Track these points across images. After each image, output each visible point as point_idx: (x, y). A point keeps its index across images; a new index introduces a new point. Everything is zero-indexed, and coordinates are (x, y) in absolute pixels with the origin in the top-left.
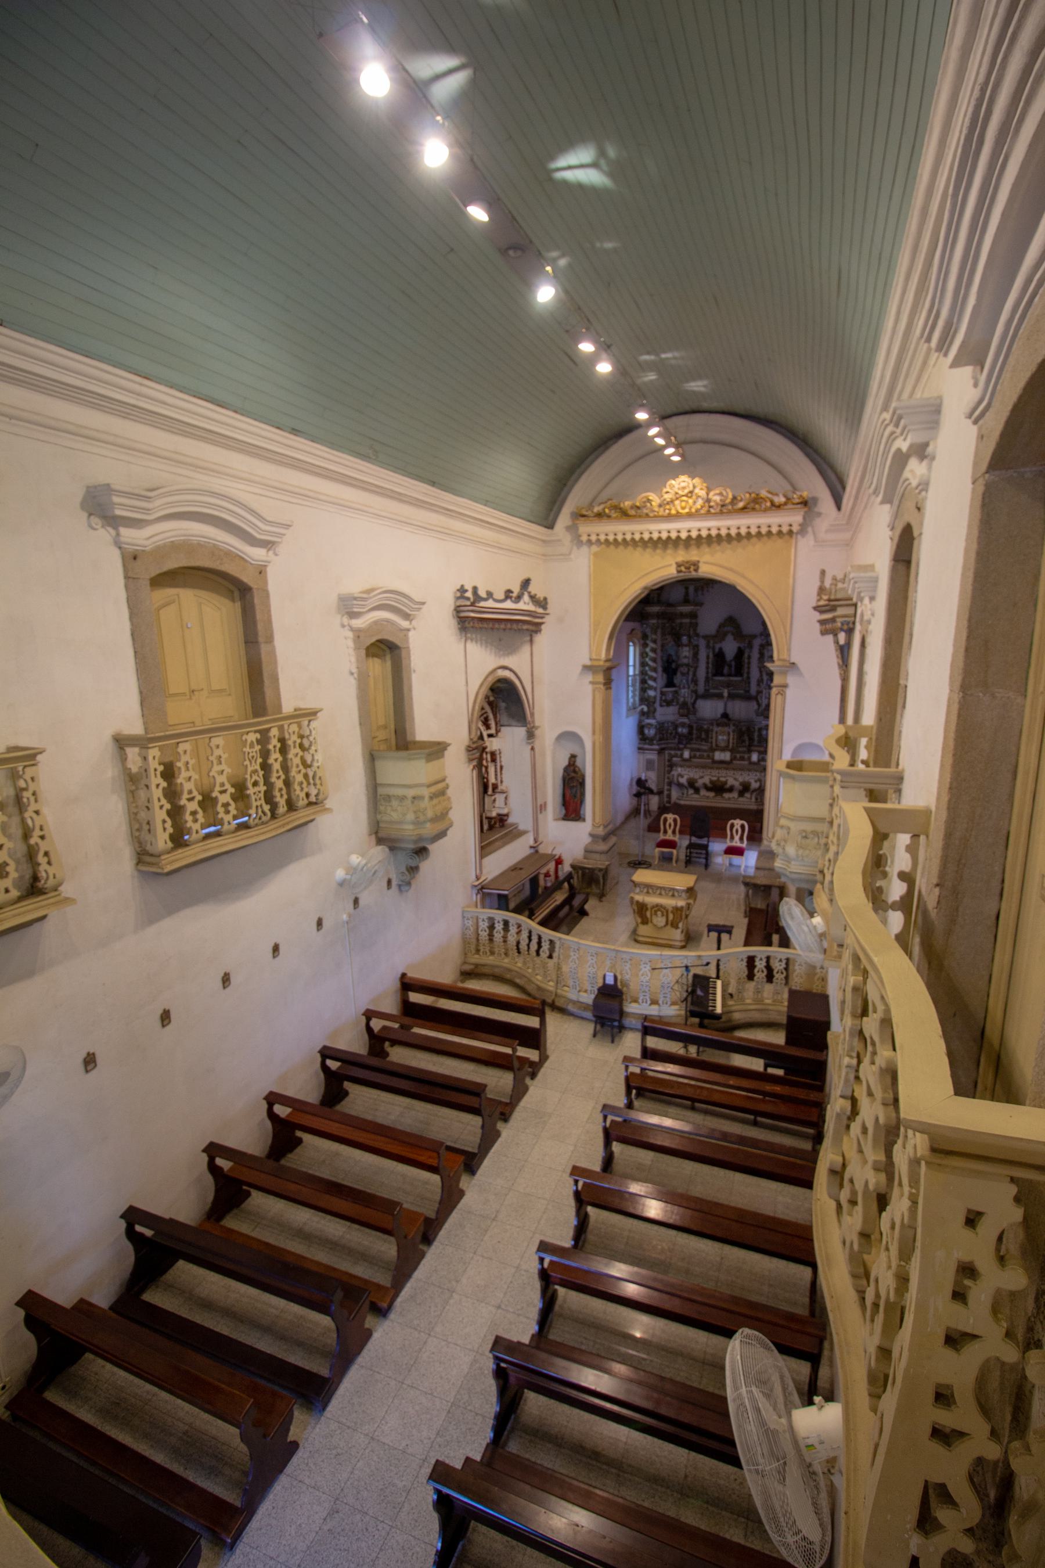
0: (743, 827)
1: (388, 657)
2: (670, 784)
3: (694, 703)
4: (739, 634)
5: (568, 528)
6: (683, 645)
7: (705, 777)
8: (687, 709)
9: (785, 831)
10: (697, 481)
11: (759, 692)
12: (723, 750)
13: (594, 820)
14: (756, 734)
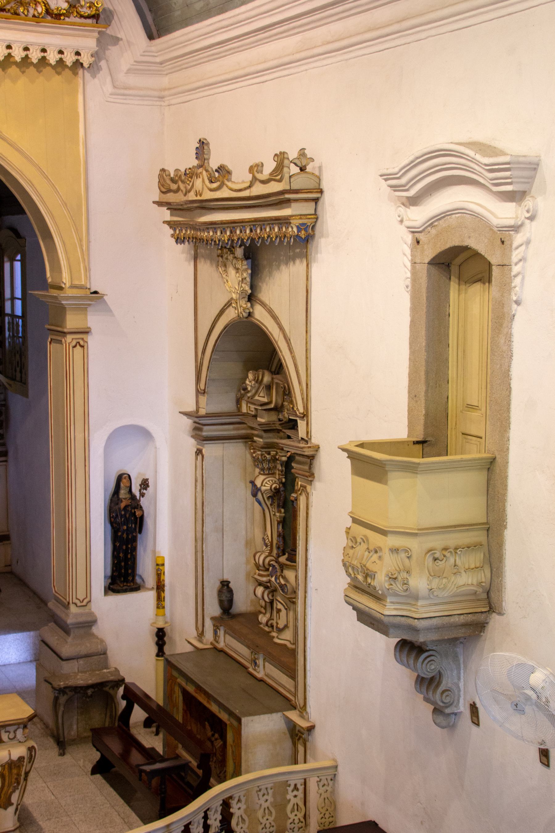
9: (403, 555)
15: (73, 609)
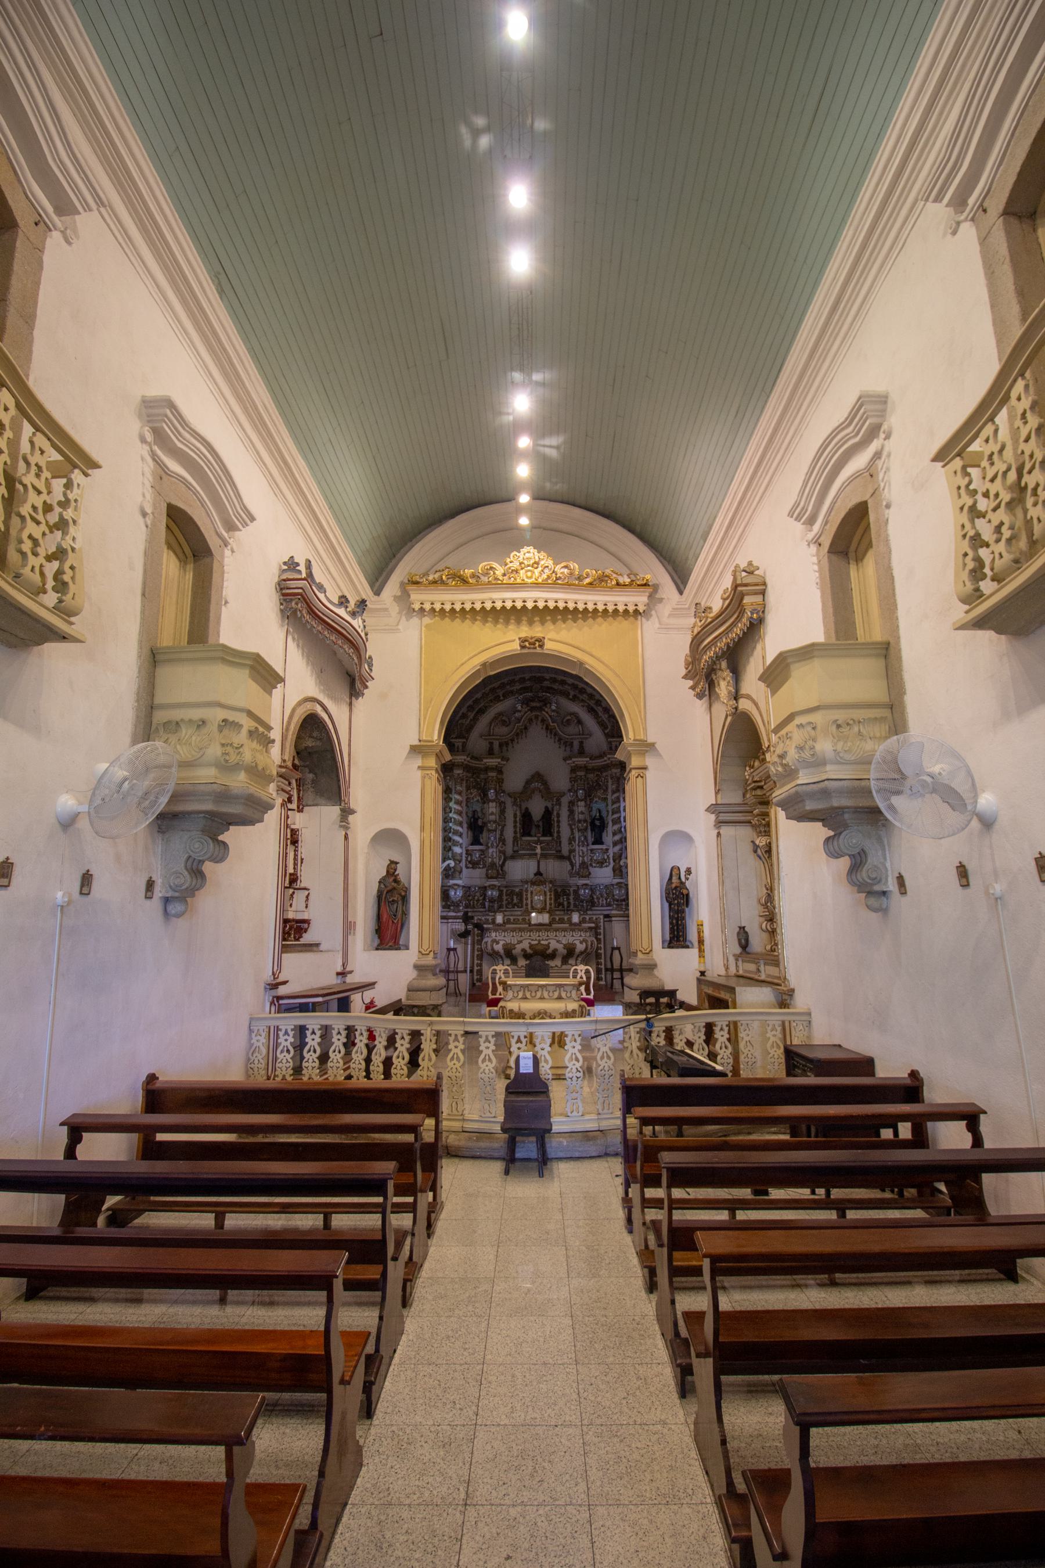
0: (587, 972)
2: (480, 958)
4: (547, 792)
7: (524, 942)
8: (497, 871)
9: (809, 729)
10: (543, 555)
11: (571, 851)
12: (540, 911)
13: (421, 944)
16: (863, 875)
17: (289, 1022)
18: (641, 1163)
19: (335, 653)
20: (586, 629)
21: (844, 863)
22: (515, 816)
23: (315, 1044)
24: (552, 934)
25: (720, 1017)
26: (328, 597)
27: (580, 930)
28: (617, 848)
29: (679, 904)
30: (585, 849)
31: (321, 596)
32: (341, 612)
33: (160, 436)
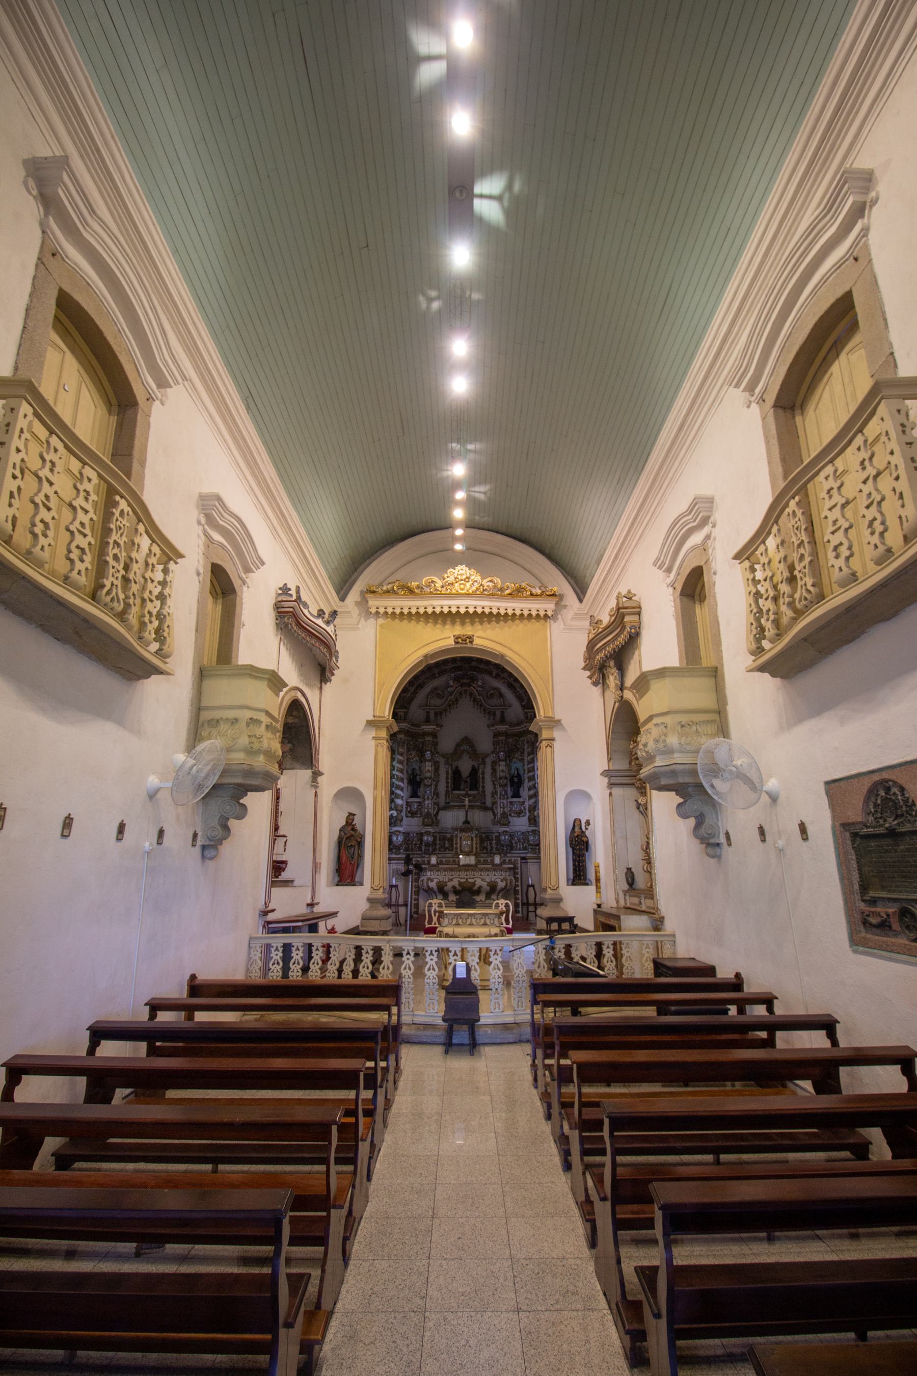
0: (507, 906)
1: (220, 601)
2: (417, 893)
3: (437, 813)
4: (474, 754)
5: (357, 604)
6: (426, 760)
7: (454, 881)
8: (431, 820)
9: (662, 727)
10: (473, 571)
12: (468, 854)
13: (373, 882)
14: (494, 842)
15: (549, 891)
16: (702, 831)
17: (278, 940)
18: (546, 1040)
19: (311, 650)
20: (506, 628)
21: (692, 822)
22: (447, 772)
23: (298, 957)
24: (477, 874)
25: (608, 938)
26: (310, 613)
27: (501, 870)
28: (532, 801)
29: (580, 849)
30: (505, 802)
31: (306, 611)
32: (319, 622)
33: (210, 520)
